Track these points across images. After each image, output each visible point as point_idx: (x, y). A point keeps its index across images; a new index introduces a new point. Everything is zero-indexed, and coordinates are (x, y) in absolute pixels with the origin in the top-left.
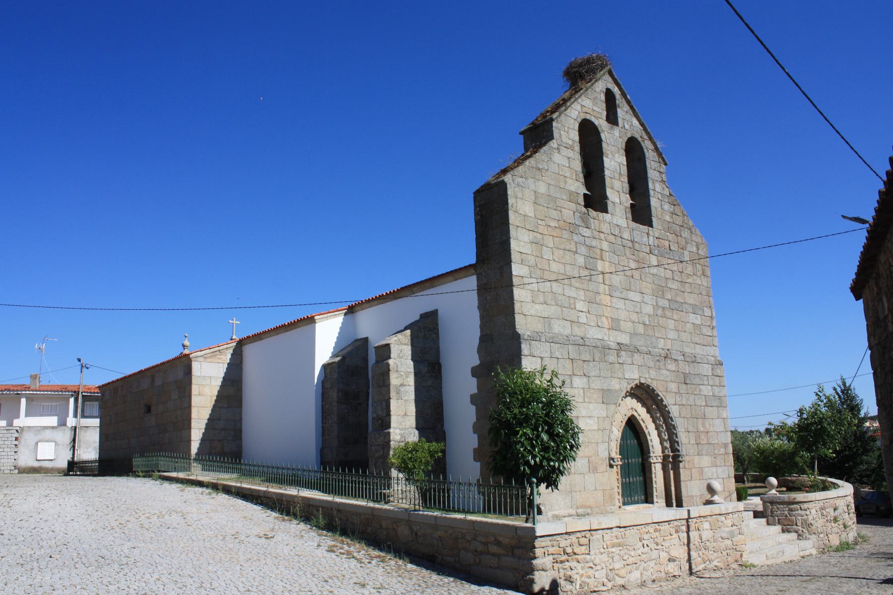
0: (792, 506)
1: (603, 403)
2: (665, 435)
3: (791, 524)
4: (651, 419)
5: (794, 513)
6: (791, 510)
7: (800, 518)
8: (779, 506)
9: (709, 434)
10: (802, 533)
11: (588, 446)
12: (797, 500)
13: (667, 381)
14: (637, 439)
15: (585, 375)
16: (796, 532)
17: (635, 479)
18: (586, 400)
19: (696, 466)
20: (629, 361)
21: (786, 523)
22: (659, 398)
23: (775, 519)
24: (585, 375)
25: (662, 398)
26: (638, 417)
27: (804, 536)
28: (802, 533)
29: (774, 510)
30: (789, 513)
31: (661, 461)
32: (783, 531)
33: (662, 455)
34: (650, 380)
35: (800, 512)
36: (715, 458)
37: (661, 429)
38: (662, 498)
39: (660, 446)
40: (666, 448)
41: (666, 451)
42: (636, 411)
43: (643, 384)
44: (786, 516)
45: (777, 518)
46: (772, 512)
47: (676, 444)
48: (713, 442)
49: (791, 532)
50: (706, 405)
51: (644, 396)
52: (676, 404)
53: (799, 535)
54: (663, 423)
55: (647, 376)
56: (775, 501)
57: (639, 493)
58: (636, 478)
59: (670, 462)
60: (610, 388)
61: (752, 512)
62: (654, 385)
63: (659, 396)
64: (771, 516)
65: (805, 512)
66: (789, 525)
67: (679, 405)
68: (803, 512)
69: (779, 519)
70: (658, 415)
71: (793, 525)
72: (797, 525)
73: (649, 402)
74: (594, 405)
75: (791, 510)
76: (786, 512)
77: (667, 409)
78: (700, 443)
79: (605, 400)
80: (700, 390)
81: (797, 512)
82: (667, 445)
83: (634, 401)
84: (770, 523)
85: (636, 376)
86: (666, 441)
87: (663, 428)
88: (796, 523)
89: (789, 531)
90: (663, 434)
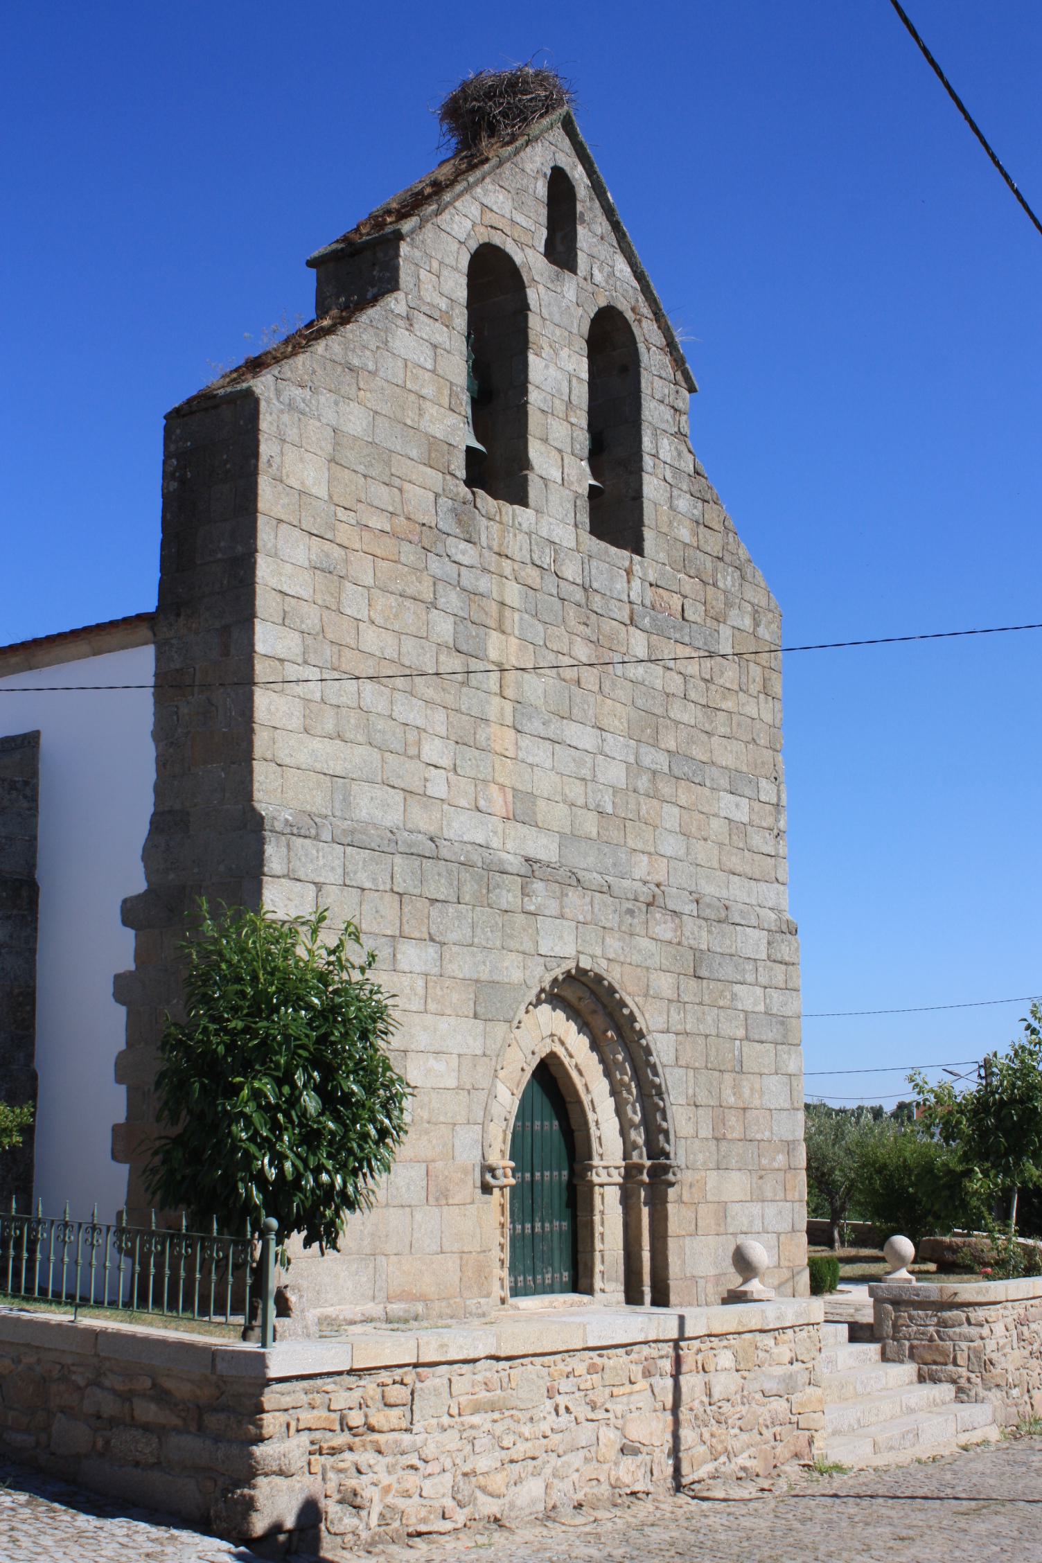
0: (947, 1314)
1: (476, 1016)
2: (635, 1112)
3: (940, 1359)
4: (601, 1067)
5: (950, 1331)
6: (943, 1324)
7: (964, 1345)
8: (914, 1313)
10: (967, 1385)
11: (427, 1132)
12: (959, 1299)
13: (648, 968)
14: (559, 1119)
15: (432, 940)
16: (954, 1382)
17: (547, 1225)
18: (432, 1006)
19: (710, 1198)
20: (553, 907)
21: (929, 1358)
22: (626, 1011)
23: (902, 1345)
24: (432, 940)
25: (632, 1012)
26: (566, 1060)
27: (972, 1393)
28: (967, 1385)
29: (901, 1322)
30: (938, 1332)
31: (620, 1180)
32: (921, 1379)
33: (623, 1163)
34: (604, 963)
35: (965, 1329)
36: (761, 1177)
37: (625, 1094)
38: (617, 1280)
39: (620, 1140)
40: (635, 1146)
41: (635, 1154)
42: (562, 1043)
43: (585, 972)
44: (931, 1340)
45: (907, 1343)
46: (896, 1327)
47: (661, 1137)
48: (759, 1137)
49: (940, 1381)
50: (747, 1038)
51: (586, 1005)
52: (668, 1031)
53: (960, 1390)
54: (631, 1080)
55: (598, 952)
56: (905, 1297)
57: (556, 1265)
58: (551, 1223)
59: (642, 1183)
60: (496, 978)
61: (846, 1326)
62: (614, 976)
63: (626, 1006)
64: (894, 1339)
65: (978, 1329)
66: (935, 1363)
67: (677, 1034)
68: (973, 1331)
69: (912, 1347)
70: (620, 1057)
71: (946, 1364)
72: (955, 1364)
73: (599, 1021)
74: (452, 1020)
75: (943, 1324)
76: (931, 1329)
77: (643, 1042)
79: (480, 1010)
80: (734, 997)
81: (957, 1330)
82: (638, 1137)
83: (560, 1015)
84: (889, 1355)
85: (570, 951)
86: (636, 1127)
87: (630, 1093)
88: (955, 1358)
89: (935, 1380)
90: (629, 1108)
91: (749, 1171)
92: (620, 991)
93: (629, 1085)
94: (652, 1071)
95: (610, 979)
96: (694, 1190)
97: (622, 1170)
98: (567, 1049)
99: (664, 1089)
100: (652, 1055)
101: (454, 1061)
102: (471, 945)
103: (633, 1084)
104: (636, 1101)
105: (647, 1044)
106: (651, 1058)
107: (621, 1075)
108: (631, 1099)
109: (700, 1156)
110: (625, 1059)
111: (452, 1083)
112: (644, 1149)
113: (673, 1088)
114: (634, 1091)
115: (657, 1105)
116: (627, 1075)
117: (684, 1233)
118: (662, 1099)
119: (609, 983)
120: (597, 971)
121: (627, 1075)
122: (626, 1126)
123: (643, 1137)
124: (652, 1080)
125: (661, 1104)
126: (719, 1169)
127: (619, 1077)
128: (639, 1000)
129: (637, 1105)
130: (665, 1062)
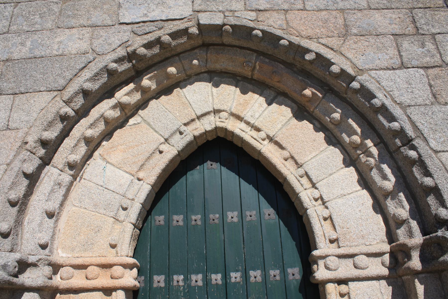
2: (385, 177)
4: (321, 135)
22: (308, 57)
25: (318, 55)
31: (385, 272)
33: (386, 247)
34: (253, 15)
37: (363, 158)
39: (379, 218)
40: (400, 223)
41: (401, 232)
42: (239, 118)
43: (218, 29)
47: (431, 200)
54: (364, 136)
59: (416, 274)
60: (37, 53)
63: (308, 51)
67: (426, 68)
70: (337, 116)
77: (355, 85)
86: (392, 194)
87: (370, 155)
90: (375, 174)
92: (285, 36)
93: (362, 147)
94: (385, 117)
95: (261, 27)
97: (387, 258)
98: (248, 123)
99: (410, 132)
100: (374, 97)
102: (8, 32)
103: (369, 143)
104: (382, 159)
105: (362, 85)
106: (375, 101)
107: (349, 136)
108: (372, 161)
110: (344, 116)
112: (414, 224)
114: (374, 151)
115: (407, 158)
116: (356, 134)
118: (414, 148)
119: (262, 31)
120: (233, 21)
121: (356, 134)
122: (381, 199)
123: (407, 207)
124: (390, 129)
125: (413, 154)
127: (347, 139)
128: (334, 42)
129: (385, 167)
130: (406, 99)
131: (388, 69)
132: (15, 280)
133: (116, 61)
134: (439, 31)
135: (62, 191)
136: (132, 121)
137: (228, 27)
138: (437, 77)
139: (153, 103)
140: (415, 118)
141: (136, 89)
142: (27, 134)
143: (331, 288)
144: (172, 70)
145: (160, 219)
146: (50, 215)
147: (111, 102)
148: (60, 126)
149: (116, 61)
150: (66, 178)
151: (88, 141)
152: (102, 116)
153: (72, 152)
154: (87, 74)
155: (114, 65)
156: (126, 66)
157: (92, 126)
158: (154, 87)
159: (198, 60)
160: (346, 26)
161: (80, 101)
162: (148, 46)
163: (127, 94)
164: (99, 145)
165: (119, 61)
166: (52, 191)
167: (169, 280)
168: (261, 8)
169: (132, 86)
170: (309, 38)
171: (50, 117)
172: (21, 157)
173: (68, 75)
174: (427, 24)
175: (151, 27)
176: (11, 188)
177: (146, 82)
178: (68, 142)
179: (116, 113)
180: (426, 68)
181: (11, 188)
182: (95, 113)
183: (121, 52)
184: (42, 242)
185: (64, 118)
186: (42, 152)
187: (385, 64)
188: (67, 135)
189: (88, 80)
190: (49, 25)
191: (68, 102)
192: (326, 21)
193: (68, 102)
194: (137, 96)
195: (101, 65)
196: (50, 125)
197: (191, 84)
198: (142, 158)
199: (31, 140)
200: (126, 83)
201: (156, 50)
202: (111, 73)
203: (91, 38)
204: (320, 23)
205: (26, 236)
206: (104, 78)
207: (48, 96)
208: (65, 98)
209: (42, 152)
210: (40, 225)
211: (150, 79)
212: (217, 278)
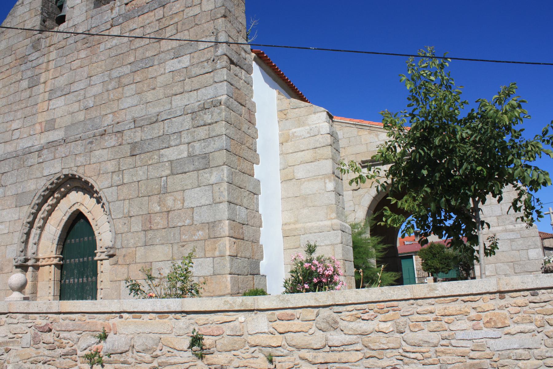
1: (16, 207)
9: (170, 214)
17: (90, 279)
19: (138, 260)
20: (51, 156)
25: (92, 185)
34: (75, 169)
36: (183, 246)
48: (179, 224)
50: (172, 174)
52: (112, 186)
55: (72, 165)
60: (24, 191)
62: (73, 171)
74: (8, 210)
78: (151, 229)
80: (160, 156)
83: (80, 193)
85: (58, 169)
91: (172, 244)
95: (77, 174)
96: (126, 258)
101: (8, 224)
109: (132, 241)
111: (6, 231)
113: (114, 211)
117: (119, 279)
126: (145, 245)
130: (109, 200)
131: (108, 188)
132: (24, 264)
133: (43, 192)
134: (125, 168)
135: (38, 236)
136: (56, 209)
137: (70, 175)
138: (120, 189)
139: (62, 201)
140: (110, 207)
141: (54, 198)
142: (23, 220)
143: (99, 262)
144: (63, 189)
145: (68, 241)
146: (35, 244)
147: (46, 205)
148: (32, 216)
149: (43, 192)
150: (39, 231)
151: (43, 218)
152: (45, 210)
153: (38, 223)
154: (36, 198)
155: (43, 193)
156: (47, 192)
157: (43, 214)
158: (59, 196)
159: (70, 185)
160: (100, 170)
161: (36, 207)
162: (51, 184)
163: (51, 200)
164: (48, 219)
165: (44, 191)
166: (34, 237)
167: (70, 261)
168: (78, 165)
169: (52, 197)
170: (90, 177)
171: (28, 214)
172: (23, 228)
173: (31, 199)
174: (122, 166)
175: (51, 177)
176: (21, 238)
177: (56, 195)
178: (37, 220)
179: (50, 207)
180: (118, 186)
181: (21, 238)
182: (43, 209)
183: (44, 188)
184: (33, 252)
185: (33, 214)
186: (29, 225)
187: (107, 186)
188: (36, 218)
189: (37, 200)
190: (26, 179)
191: (33, 208)
192: (94, 169)
193: (33, 208)
194: (55, 200)
195: (39, 194)
196: (29, 217)
197: (71, 192)
198: (58, 222)
199: (25, 222)
200: (50, 197)
201: (54, 185)
202: (44, 196)
203: (37, 183)
204: (93, 170)
205: (29, 251)
206: (42, 198)
207: (27, 207)
208: (32, 207)
209: (29, 225)
210: (32, 247)
211: (57, 194)
212: (81, 260)
